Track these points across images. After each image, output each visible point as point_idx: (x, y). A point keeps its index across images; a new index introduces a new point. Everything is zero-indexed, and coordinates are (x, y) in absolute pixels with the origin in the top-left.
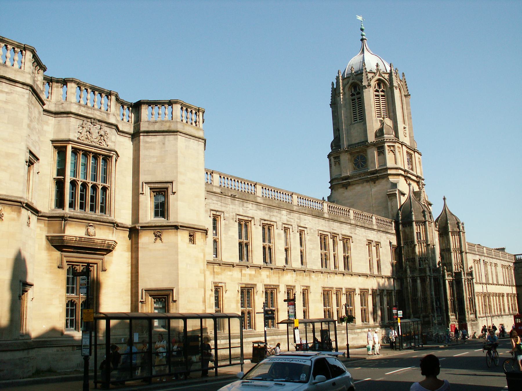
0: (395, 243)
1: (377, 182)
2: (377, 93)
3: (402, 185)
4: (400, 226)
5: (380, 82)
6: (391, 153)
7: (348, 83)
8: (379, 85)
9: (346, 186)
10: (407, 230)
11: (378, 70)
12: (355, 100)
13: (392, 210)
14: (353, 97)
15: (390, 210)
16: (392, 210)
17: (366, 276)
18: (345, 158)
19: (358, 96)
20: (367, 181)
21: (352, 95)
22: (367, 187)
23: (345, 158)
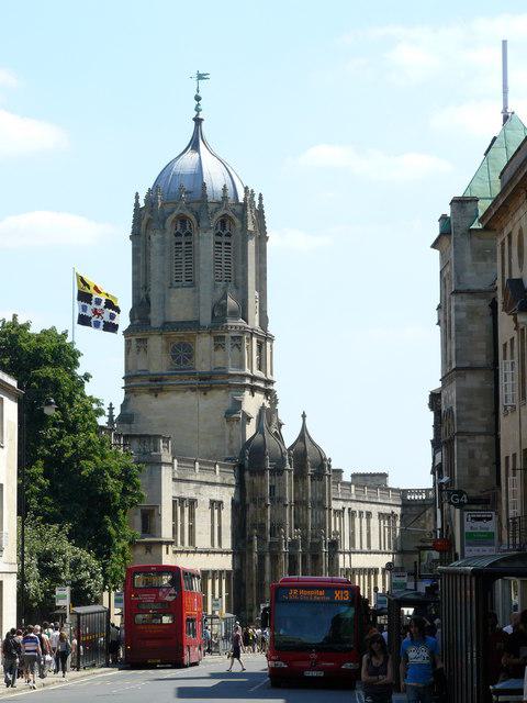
0: (237, 499)
1: (208, 393)
2: (219, 239)
3: (252, 404)
4: (247, 474)
5: (223, 221)
6: (236, 349)
7: (171, 213)
8: (223, 223)
9: (156, 392)
10: (257, 480)
11: (225, 198)
12: (180, 243)
13: (231, 442)
14: (179, 239)
15: (228, 442)
16: (231, 442)
17: (207, 553)
18: (156, 343)
19: (188, 239)
20: (193, 390)
21: (177, 235)
22: (192, 399)
23: (156, 343)
